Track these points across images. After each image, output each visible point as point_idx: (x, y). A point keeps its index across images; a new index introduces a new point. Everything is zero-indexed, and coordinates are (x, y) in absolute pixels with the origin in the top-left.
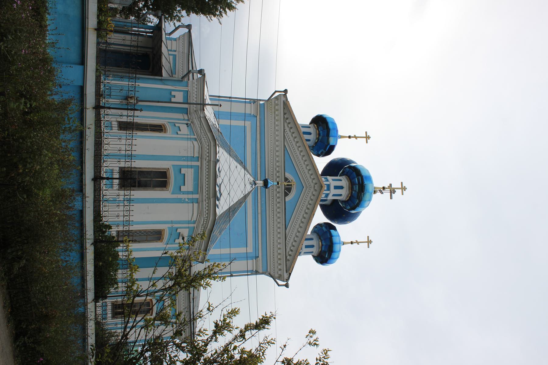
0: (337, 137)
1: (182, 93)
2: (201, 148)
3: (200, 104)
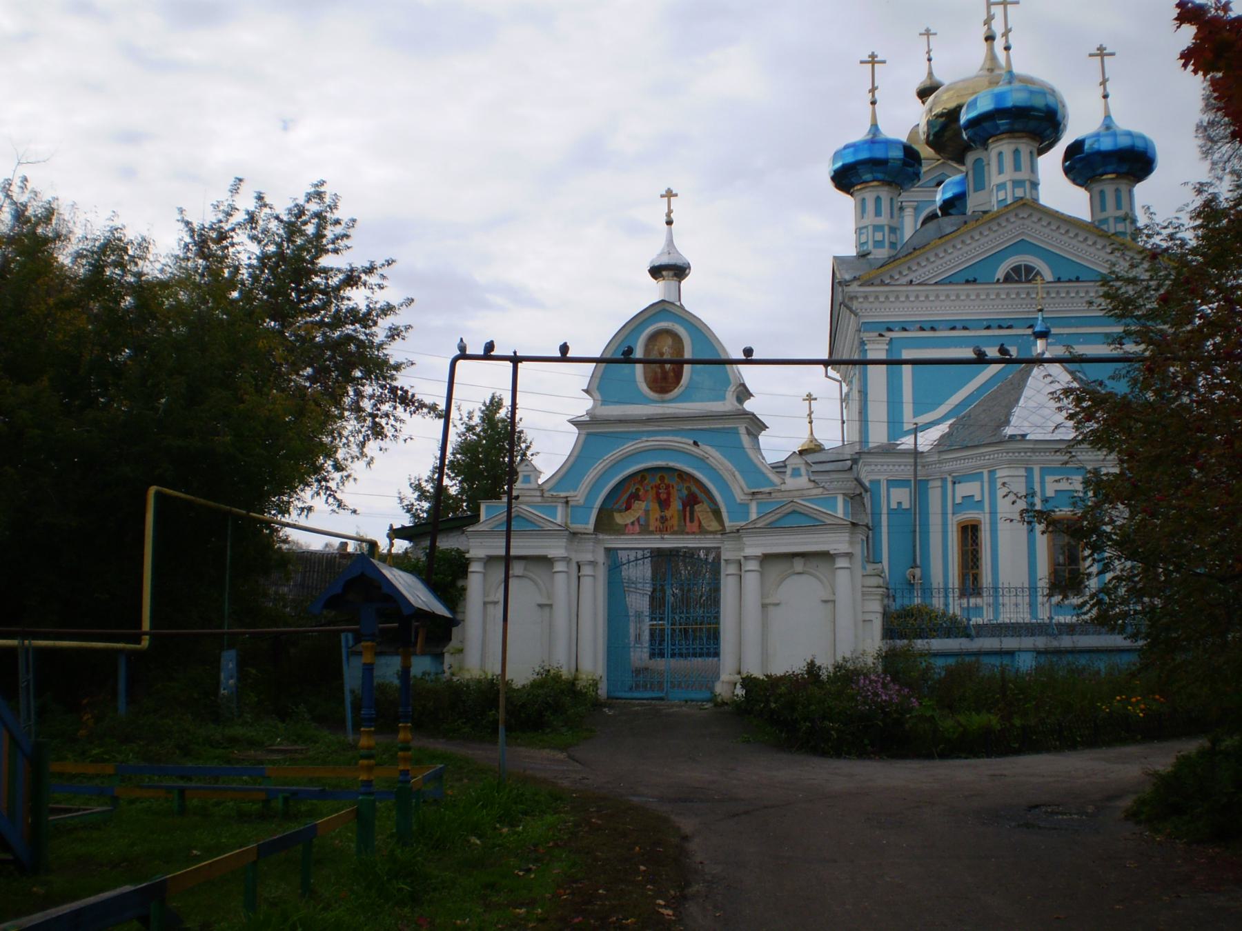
0: (875, 138)
1: (892, 490)
2: (1011, 463)
3: (916, 458)
